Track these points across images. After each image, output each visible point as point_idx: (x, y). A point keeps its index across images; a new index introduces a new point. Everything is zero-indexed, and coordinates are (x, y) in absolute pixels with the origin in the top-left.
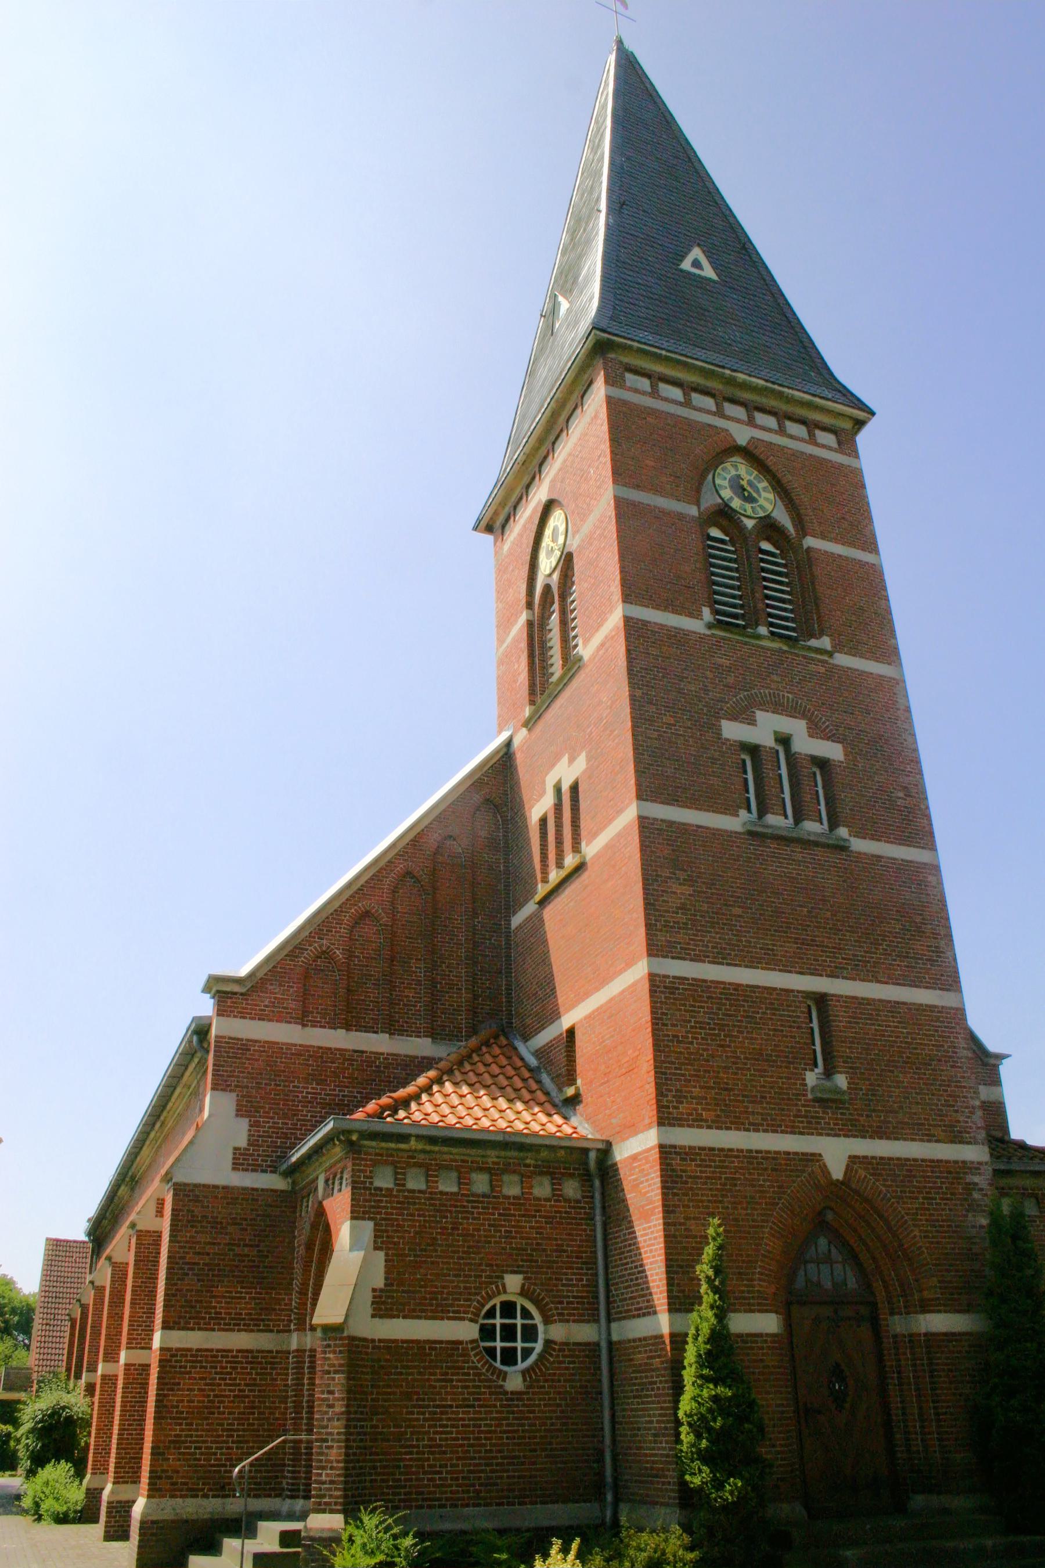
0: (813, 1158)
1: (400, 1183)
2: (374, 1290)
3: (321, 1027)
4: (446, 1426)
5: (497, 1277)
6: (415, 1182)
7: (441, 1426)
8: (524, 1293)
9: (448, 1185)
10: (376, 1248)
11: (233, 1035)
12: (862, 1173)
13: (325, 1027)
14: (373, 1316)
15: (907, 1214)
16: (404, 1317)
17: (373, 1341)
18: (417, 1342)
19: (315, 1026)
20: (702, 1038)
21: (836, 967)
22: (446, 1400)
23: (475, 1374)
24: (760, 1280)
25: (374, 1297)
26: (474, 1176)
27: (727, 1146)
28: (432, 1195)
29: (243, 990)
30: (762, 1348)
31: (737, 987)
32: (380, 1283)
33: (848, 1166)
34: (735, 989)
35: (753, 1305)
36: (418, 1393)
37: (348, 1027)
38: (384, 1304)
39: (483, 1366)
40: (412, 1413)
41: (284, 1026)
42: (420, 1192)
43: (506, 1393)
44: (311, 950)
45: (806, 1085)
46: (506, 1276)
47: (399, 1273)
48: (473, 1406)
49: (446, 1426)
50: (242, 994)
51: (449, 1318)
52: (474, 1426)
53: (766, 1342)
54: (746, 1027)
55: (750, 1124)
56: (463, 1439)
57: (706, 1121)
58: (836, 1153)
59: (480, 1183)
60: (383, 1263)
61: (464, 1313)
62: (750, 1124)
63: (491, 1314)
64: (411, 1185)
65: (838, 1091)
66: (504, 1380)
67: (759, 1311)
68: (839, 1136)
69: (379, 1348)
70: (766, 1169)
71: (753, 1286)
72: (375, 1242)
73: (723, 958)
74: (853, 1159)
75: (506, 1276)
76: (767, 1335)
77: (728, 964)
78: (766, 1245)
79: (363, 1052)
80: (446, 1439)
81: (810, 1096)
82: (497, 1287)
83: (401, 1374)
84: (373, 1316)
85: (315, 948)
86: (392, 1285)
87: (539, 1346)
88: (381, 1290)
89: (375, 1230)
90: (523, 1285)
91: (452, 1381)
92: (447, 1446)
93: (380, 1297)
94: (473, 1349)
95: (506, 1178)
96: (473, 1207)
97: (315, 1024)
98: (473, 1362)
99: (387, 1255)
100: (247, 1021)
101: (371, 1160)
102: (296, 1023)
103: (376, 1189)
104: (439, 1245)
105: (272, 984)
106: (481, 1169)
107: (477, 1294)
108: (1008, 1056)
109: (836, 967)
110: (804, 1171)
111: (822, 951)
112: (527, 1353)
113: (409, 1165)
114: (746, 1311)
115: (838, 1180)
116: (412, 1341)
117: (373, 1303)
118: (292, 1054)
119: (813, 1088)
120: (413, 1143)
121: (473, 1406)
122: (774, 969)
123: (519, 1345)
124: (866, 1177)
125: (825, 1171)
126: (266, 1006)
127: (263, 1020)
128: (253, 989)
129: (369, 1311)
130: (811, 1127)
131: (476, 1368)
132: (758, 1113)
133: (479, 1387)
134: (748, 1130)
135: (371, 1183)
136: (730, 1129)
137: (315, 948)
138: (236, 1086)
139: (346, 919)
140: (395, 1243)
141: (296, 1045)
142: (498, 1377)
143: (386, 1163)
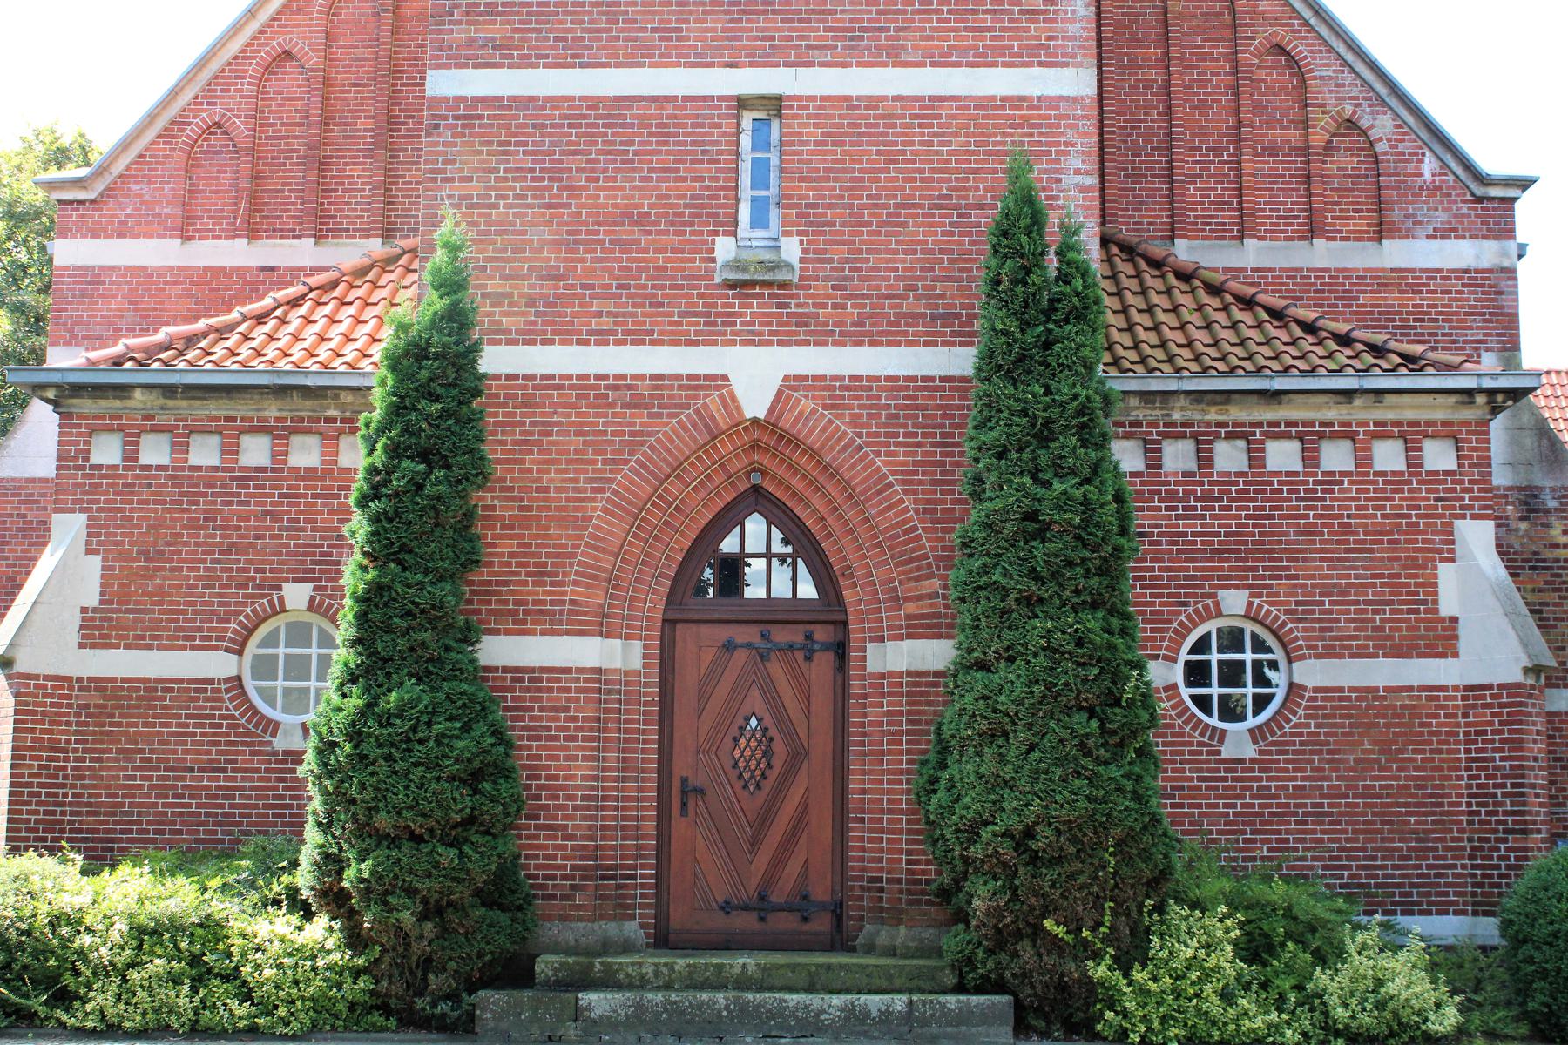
1: (130, 458)
2: (84, 610)
3: (215, 238)
4: (183, 796)
5: (272, 588)
6: (155, 452)
7: (175, 796)
8: (311, 606)
9: (205, 453)
10: (89, 552)
11: (79, 263)
12: (807, 405)
13: (219, 238)
14: (81, 646)
15: (894, 473)
16: (127, 647)
17: (80, 680)
18: (146, 680)
19: (207, 238)
20: (517, 197)
21: (809, 47)
22: (184, 760)
23: (229, 726)
24: (576, 583)
25: (83, 619)
26: (247, 441)
28: (179, 471)
29: (92, 195)
30: (568, 690)
31: (593, 103)
32: (93, 601)
33: (779, 394)
34: (589, 108)
35: (561, 622)
36: (142, 751)
37: (253, 233)
38: (97, 630)
39: (242, 715)
40: (133, 778)
41: (154, 243)
42: (159, 468)
43: (276, 753)
44: (198, 123)
45: (714, 260)
46: (284, 585)
47: (122, 585)
48: (224, 770)
49: (183, 796)
50: (93, 202)
51: (194, 648)
52: (225, 797)
53: (577, 680)
54: (605, 170)
55: (590, 333)
56: (207, 815)
57: (507, 331)
58: (755, 375)
59: (256, 451)
60: (98, 572)
61: (219, 639)
62: (590, 333)
64: (146, 458)
65: (776, 266)
66: (274, 735)
67: (569, 633)
68: (769, 343)
69: (88, 689)
70: (611, 405)
71: (564, 593)
72: (88, 543)
73: (574, 56)
74: (792, 383)
75: (284, 585)
76: (580, 670)
77: (582, 66)
78: (596, 527)
79: (272, 269)
80: (181, 814)
81: (718, 280)
82: (271, 602)
83: (119, 724)
84: (81, 646)
85: (203, 120)
86: (111, 602)
88: (94, 610)
89: (88, 526)
90: (312, 599)
91: (194, 734)
92: (183, 823)
93: (93, 619)
94: (228, 691)
95: (296, 440)
96: (239, 487)
97: (204, 234)
98: (228, 709)
99: (104, 560)
100: (101, 241)
101: (87, 426)
102: (171, 236)
103: (93, 467)
104: (186, 544)
105: (137, 183)
106: (254, 430)
107: (238, 613)
108: (1525, 184)
109: (809, 47)
110: (688, 406)
111: (783, 21)
113: (143, 430)
114: (543, 633)
115: (755, 421)
116: (138, 680)
117: (82, 627)
118: (166, 283)
119: (726, 265)
120: (138, 394)
121: (224, 770)
122: (678, 65)
123: (281, 683)
124: (814, 411)
126: (127, 216)
127: (124, 236)
128: (110, 191)
129: (75, 638)
130: (713, 328)
131: (233, 717)
132: (609, 314)
133: (234, 743)
134: (586, 343)
135: (87, 459)
136: (551, 342)
137: (203, 120)
138: (84, 337)
139: (252, 69)
140: (116, 543)
141: (172, 269)
142: (265, 731)
143: (110, 430)
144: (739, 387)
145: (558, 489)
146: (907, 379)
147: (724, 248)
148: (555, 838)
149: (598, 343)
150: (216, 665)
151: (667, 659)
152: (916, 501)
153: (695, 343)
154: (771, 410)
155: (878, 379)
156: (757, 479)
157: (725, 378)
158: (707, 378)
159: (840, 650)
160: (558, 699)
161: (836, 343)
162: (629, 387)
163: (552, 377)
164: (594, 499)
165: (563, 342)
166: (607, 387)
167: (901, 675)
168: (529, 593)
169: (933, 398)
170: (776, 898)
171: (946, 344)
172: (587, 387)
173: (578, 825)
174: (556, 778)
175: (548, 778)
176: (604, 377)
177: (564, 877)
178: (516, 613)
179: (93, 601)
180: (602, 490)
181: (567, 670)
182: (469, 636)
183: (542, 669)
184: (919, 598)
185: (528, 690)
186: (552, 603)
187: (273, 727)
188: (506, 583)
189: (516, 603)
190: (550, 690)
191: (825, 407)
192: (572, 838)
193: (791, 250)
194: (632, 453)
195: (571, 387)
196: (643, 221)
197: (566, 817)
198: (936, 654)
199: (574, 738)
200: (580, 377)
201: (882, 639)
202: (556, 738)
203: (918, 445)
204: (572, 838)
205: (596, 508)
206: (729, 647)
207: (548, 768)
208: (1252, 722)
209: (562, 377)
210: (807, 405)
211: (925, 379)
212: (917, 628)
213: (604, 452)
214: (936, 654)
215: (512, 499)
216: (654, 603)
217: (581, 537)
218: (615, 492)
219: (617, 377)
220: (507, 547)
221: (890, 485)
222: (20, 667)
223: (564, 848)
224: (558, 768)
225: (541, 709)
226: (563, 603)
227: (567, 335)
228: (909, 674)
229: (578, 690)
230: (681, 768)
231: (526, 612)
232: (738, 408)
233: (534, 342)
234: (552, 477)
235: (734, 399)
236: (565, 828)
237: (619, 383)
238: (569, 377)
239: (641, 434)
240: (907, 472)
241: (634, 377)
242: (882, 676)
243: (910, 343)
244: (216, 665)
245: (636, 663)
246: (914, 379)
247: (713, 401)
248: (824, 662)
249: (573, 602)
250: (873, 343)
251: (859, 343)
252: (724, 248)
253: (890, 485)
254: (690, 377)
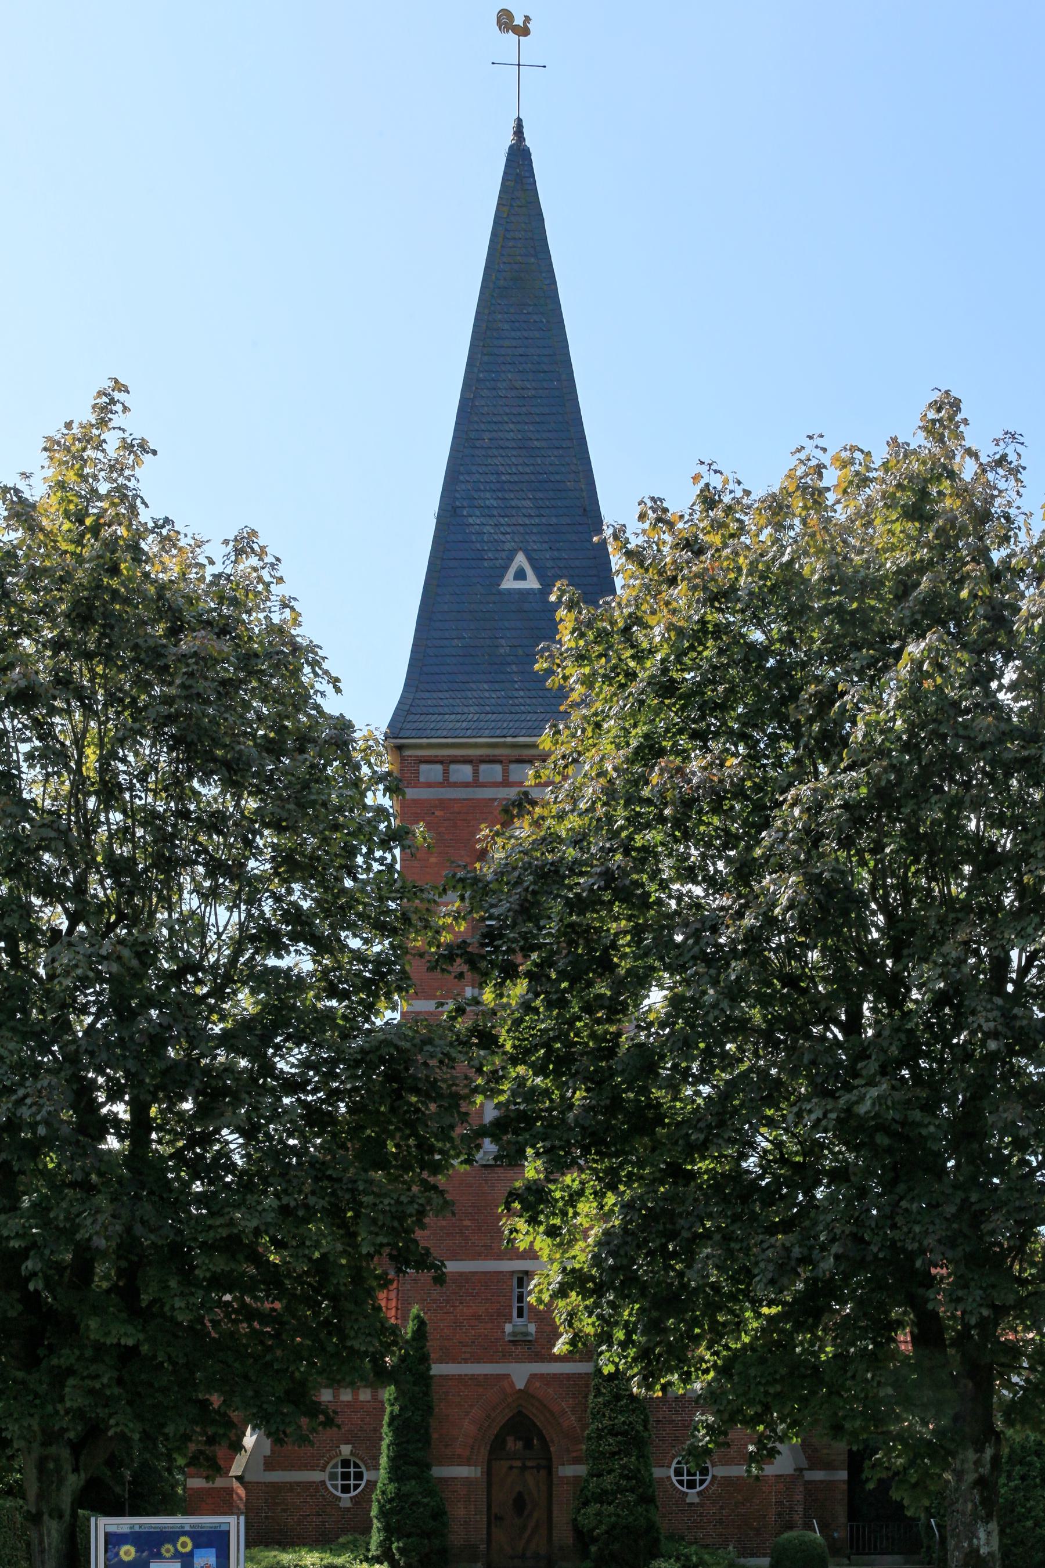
0: (507, 1376)
8: (352, 1454)
12: (538, 1384)
32: (268, 1453)
38: (270, 1464)
63: (356, 1466)
65: (527, 1334)
74: (533, 1376)
87: (363, 1483)
112: (356, 1487)
129: (262, 1467)
130: (505, 1357)
144: (514, 1378)
147: (508, 1328)
150: (316, 1476)
151: (489, 1473)
172: (460, 1378)
179: (268, 1453)
182: (428, 1467)
187: (339, 1499)
193: (532, 1328)
196: (478, 1318)
198: (581, 1470)
208: (699, 1489)
210: (538, 1384)
212: (576, 1461)
214: (581, 1470)
216: (484, 1452)
222: (247, 1478)
227: (454, 1360)
237: (473, 1377)
244: (316, 1476)
245: (479, 1474)
248: (543, 1472)
252: (508, 1328)
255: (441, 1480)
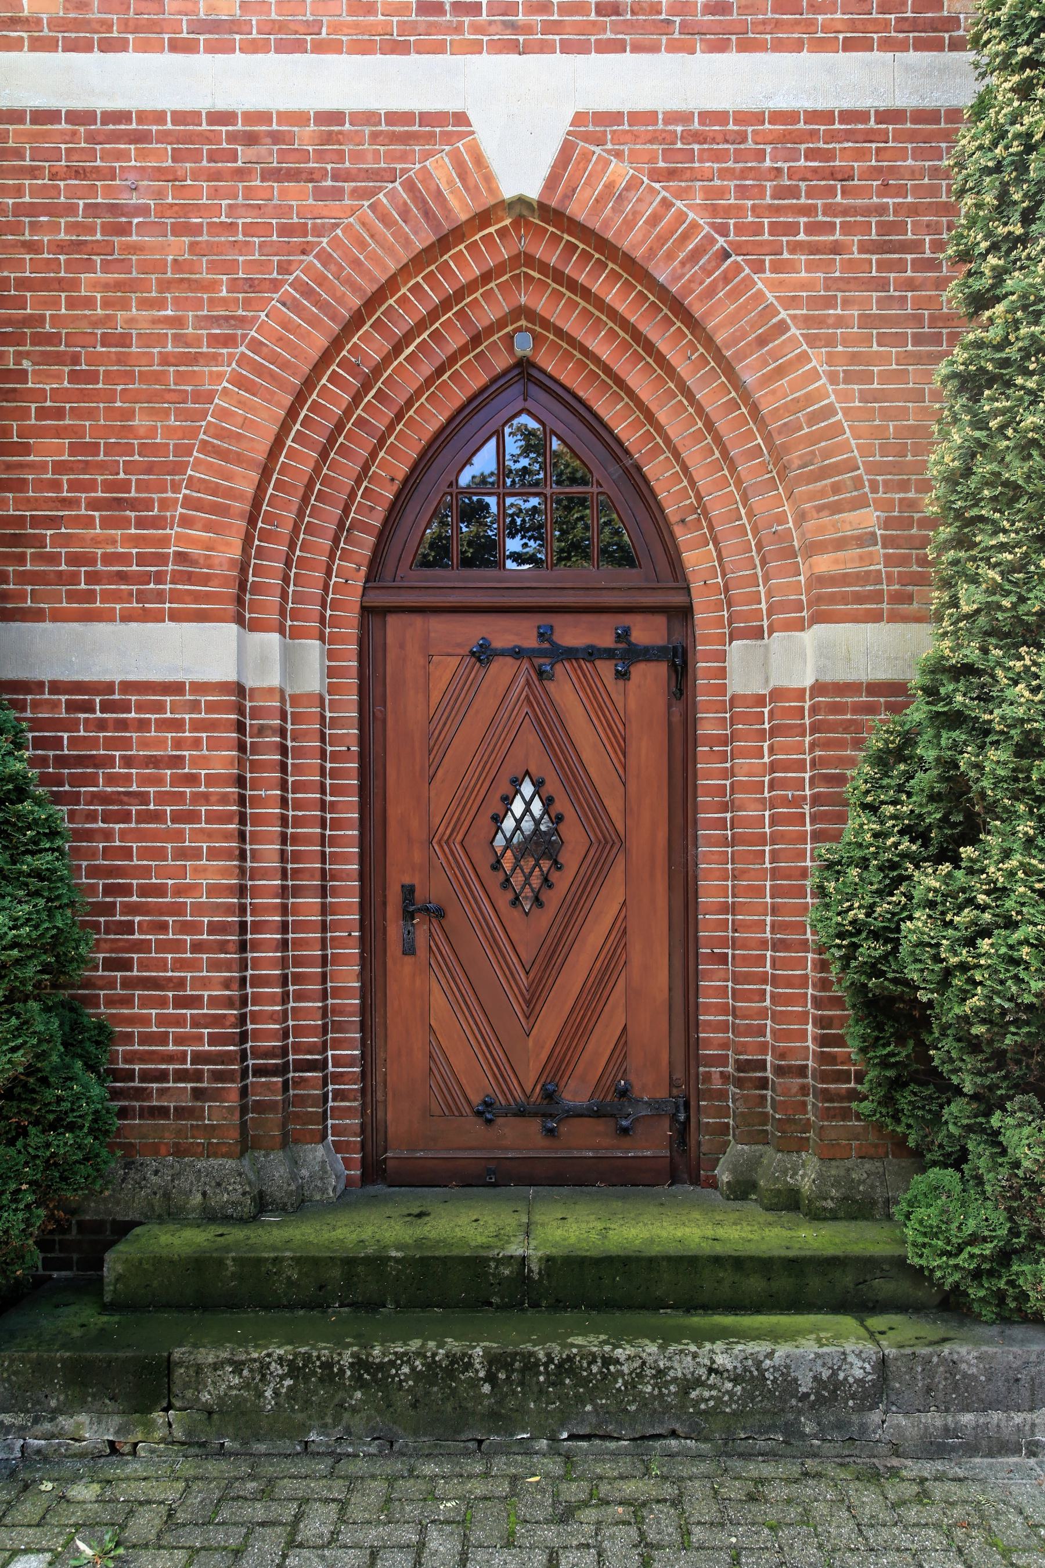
0: (449, 125)
15: (791, 302)
24: (186, 522)
27: (101, 104)
30: (177, 725)
33: (566, 150)
35: (160, 597)
53: (195, 706)
67: (176, 616)
71: (165, 541)
74: (593, 128)
76: (199, 687)
78: (223, 414)
114: (127, 617)
124: (633, 184)
125: (473, 168)
136: (120, 46)
144: (489, 135)
145: (148, 340)
146: (815, 116)
148: (162, 1003)
149: (212, 49)
152: (830, 359)
153: (399, 48)
154: (552, 181)
155: (757, 117)
156: (524, 345)
157: (461, 118)
158: (426, 118)
159: (679, 662)
160: (161, 743)
161: (674, 47)
162: (276, 138)
163: (123, 116)
164: (214, 359)
165: (144, 47)
166: (232, 137)
167: (799, 694)
168: (96, 542)
169: (861, 155)
170: (576, 1093)
171: (887, 45)
173: (208, 981)
174: (160, 890)
175: (144, 891)
176: (224, 117)
177: (182, 1076)
178: (74, 578)
180: (229, 341)
181: (175, 688)
183: (128, 687)
184: (840, 544)
185: (102, 725)
186: (142, 559)
188: (53, 522)
189: (74, 559)
190: (143, 725)
191: (656, 175)
192: (194, 1002)
194: (284, 268)
195: (164, 137)
197: (181, 965)
199: (192, 817)
200: (180, 117)
201: (757, 634)
202: (157, 817)
203: (836, 248)
204: (194, 1002)
205: (220, 375)
206: (483, 654)
207: (146, 872)
209: (143, 116)
210: (620, 171)
211: (848, 116)
213: (230, 267)
215: (59, 358)
217: (194, 433)
218: (255, 346)
219: (253, 117)
220: (50, 451)
221: (782, 327)
223: (179, 1021)
224: (161, 872)
225: (128, 762)
226: (163, 559)
228: (819, 688)
229: (196, 725)
230: (400, 873)
231: (93, 578)
232: (489, 179)
233: (86, 47)
234: (133, 316)
235: (479, 160)
236: (181, 983)
237: (254, 128)
238: (159, 117)
239: (303, 230)
240: (814, 302)
241: (286, 117)
242: (760, 700)
243: (820, 46)
246: (825, 116)
247: (440, 169)
248: (650, 679)
249: (181, 558)
250: (745, 46)
251: (721, 47)
253: (782, 327)
254: (393, 118)
255: (82, 693)
